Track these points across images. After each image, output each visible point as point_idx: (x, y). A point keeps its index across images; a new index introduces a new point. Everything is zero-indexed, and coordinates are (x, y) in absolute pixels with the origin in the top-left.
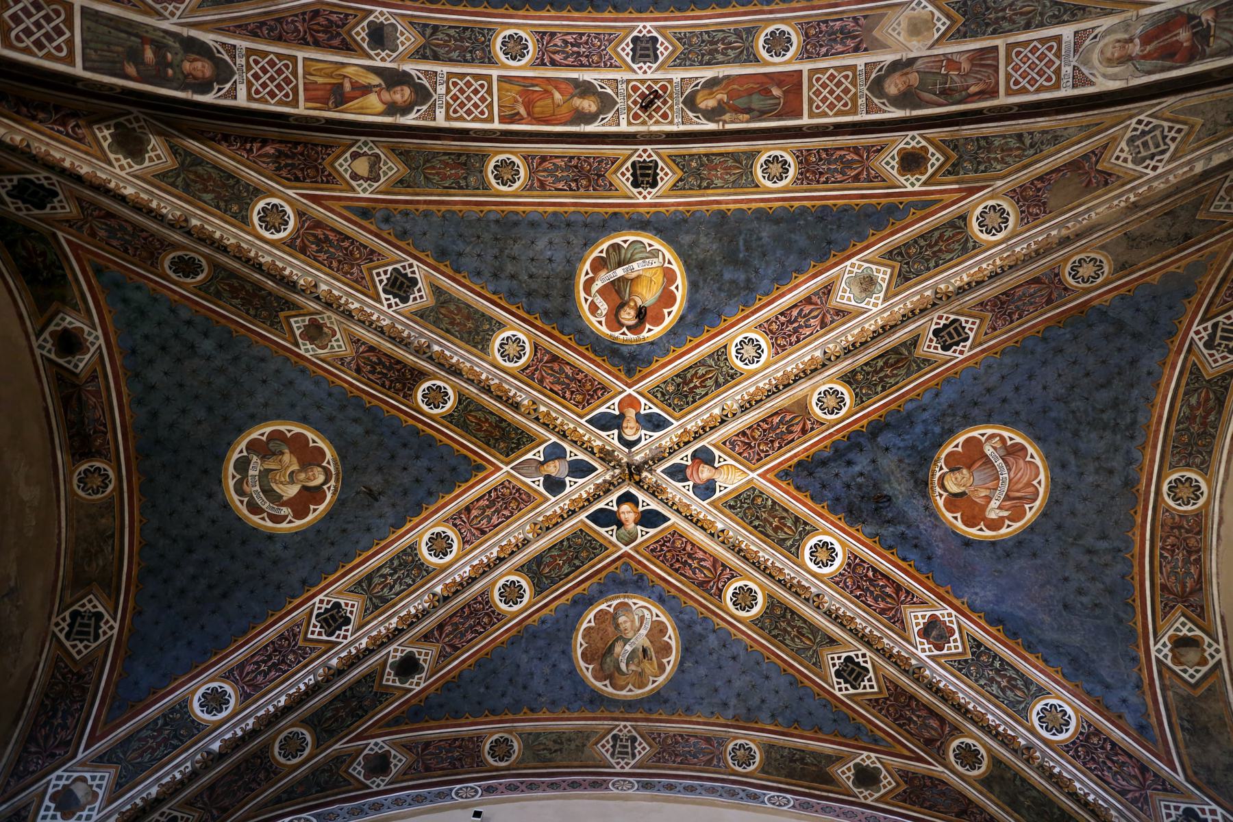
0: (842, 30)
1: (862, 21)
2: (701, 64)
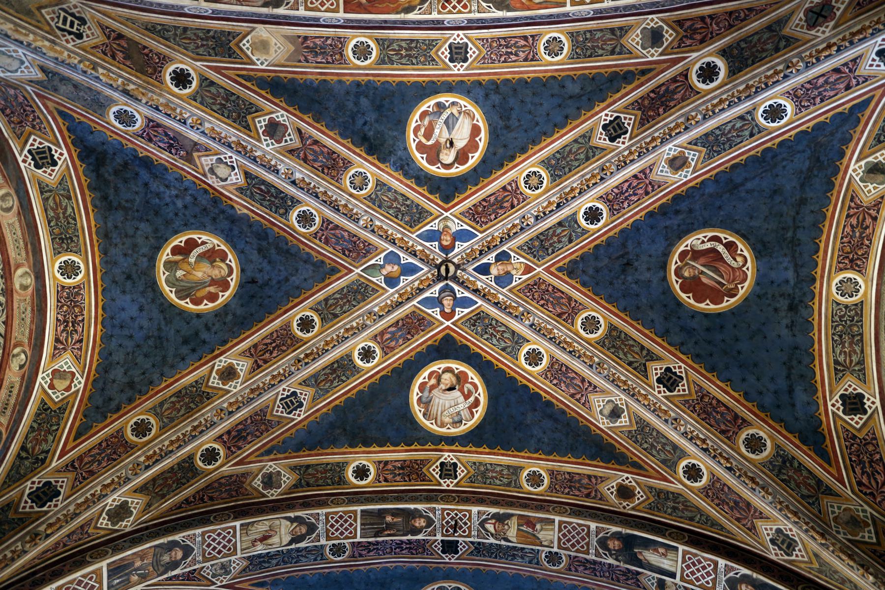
0: (316, 55)
1: (302, 59)
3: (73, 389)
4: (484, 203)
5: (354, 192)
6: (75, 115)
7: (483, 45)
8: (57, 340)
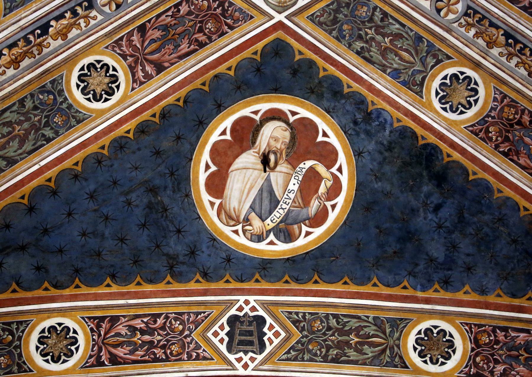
2: (325, 359)
4: (202, 38)
5: (470, 72)
7: (198, 347)
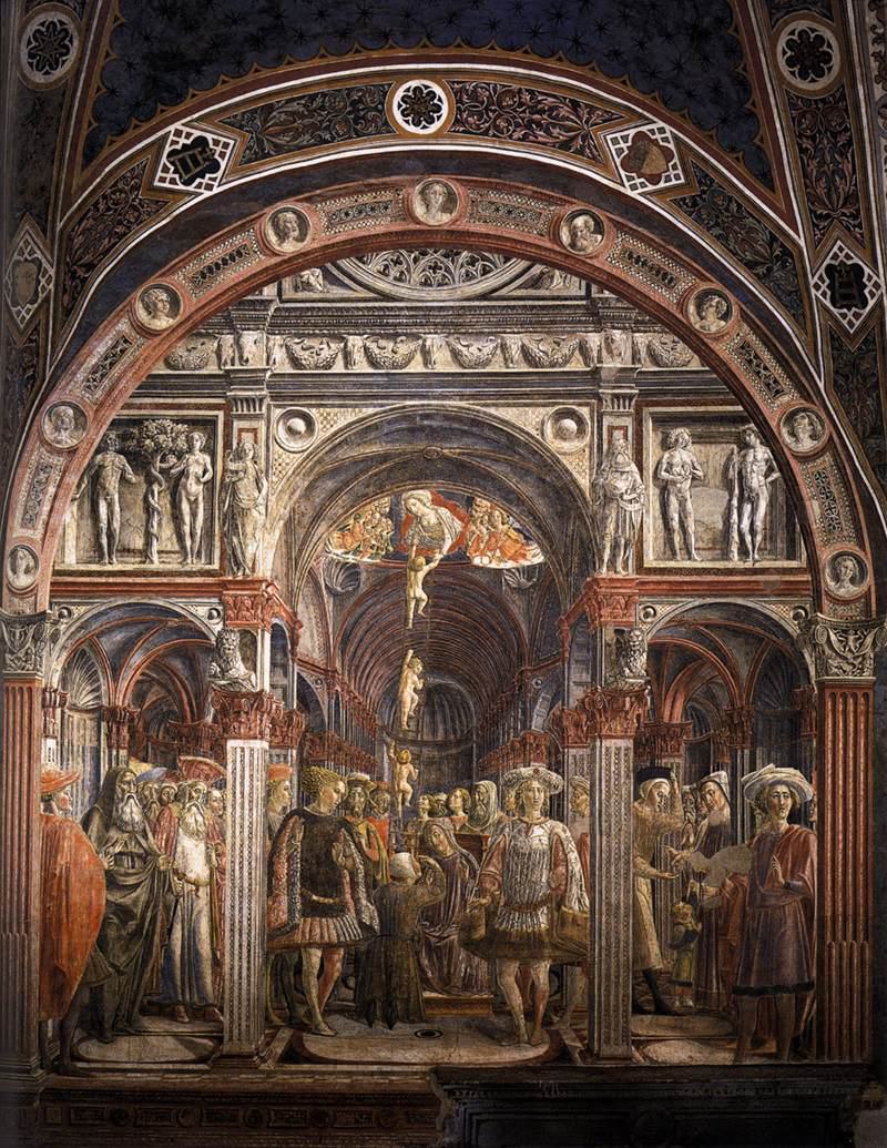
3: (671, 146)
6: (85, 132)
8: (565, 146)
